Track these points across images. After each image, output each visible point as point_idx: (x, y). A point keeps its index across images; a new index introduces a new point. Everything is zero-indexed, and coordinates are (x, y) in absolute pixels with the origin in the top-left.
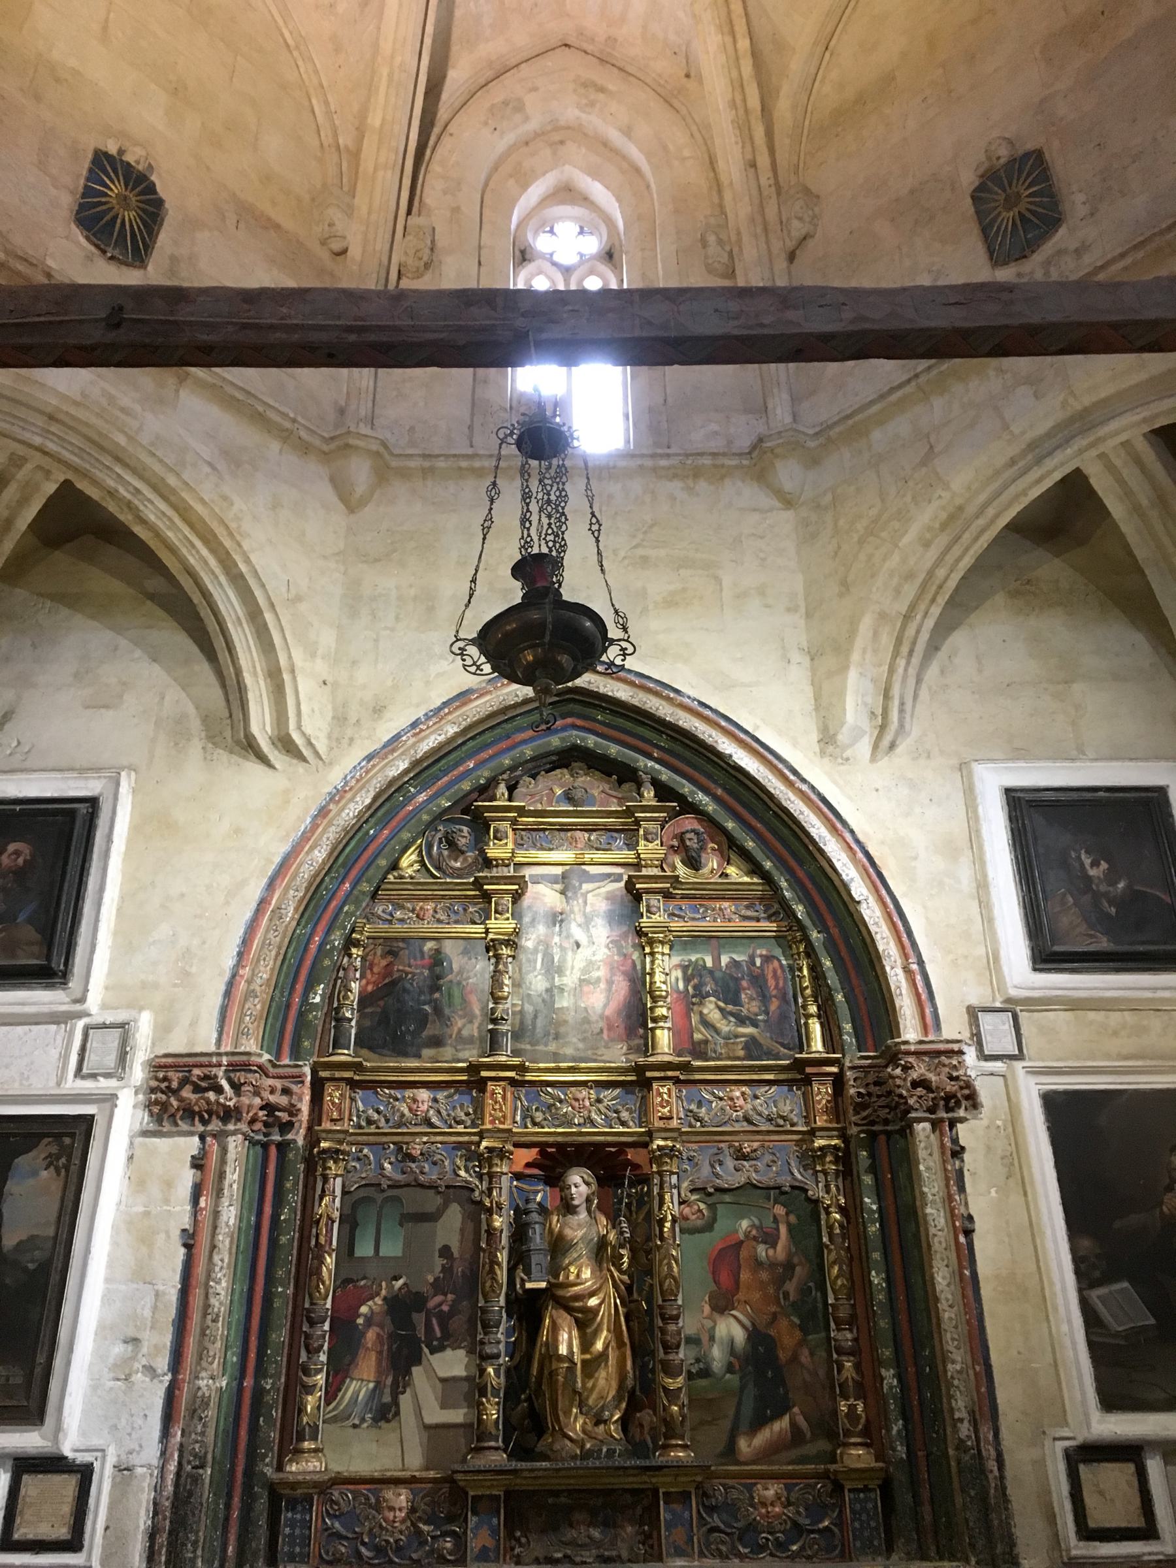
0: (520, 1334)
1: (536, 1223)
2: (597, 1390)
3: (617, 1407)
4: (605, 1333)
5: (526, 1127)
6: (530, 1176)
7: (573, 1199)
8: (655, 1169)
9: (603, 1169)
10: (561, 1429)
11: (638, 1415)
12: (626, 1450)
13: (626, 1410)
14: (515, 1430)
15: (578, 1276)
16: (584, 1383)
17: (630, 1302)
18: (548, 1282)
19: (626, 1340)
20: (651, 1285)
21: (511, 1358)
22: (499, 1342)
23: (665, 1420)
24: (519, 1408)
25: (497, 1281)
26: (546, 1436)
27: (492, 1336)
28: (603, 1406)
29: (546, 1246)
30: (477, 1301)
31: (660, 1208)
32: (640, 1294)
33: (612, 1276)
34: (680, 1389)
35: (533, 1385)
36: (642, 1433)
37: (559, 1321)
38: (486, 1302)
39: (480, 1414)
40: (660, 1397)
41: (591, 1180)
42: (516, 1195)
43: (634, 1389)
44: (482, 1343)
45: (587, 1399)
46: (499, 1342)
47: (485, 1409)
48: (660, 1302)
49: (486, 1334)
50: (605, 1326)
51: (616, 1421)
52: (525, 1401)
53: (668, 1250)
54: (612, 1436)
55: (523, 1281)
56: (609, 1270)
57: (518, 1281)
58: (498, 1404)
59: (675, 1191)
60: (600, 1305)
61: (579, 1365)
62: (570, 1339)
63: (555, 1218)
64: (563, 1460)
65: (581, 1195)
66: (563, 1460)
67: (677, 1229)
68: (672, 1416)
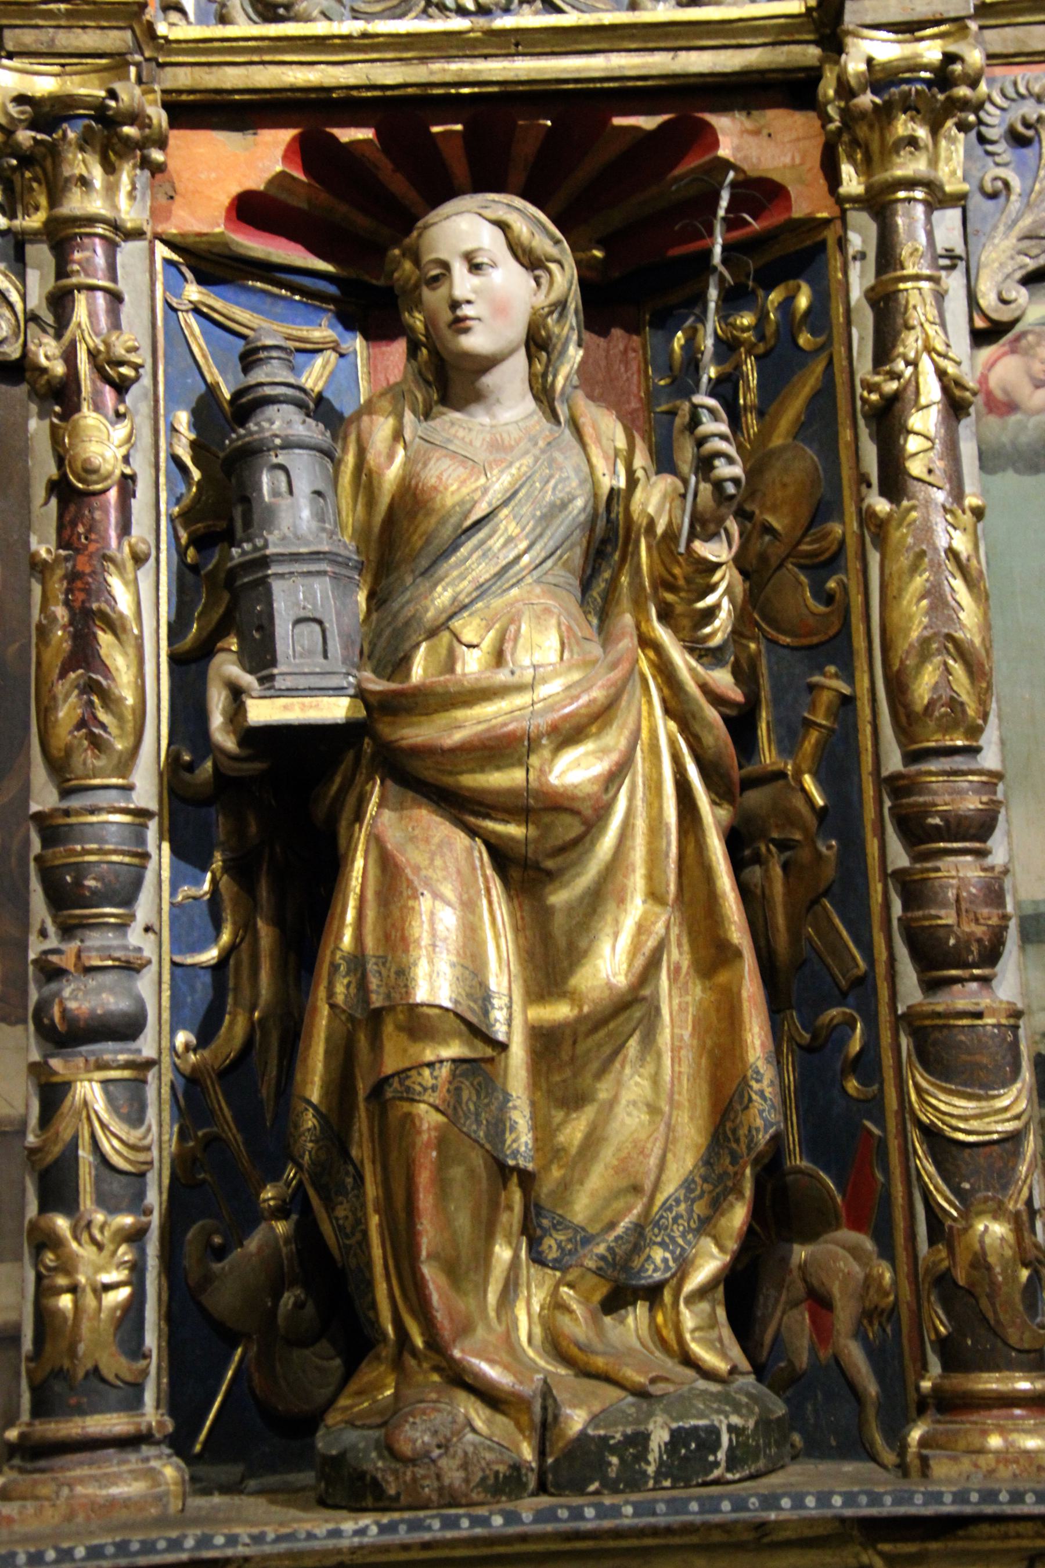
0: (246, 928)
1: (289, 445)
2: (608, 1155)
3: (705, 1226)
4: (636, 907)
5: (223, 19)
6: (266, 270)
7: (459, 325)
8: (852, 182)
9: (600, 244)
10: (436, 1345)
11: (801, 1253)
12: (765, 1424)
13: (750, 1238)
14: (231, 1339)
15: (499, 657)
16: (543, 1130)
17: (749, 783)
18: (361, 694)
19: (738, 933)
20: (847, 702)
21: (205, 1035)
22: (131, 967)
23: (943, 1281)
24: (253, 1244)
25: (109, 699)
26: (368, 1373)
27: (95, 939)
28: (639, 1228)
29: (347, 544)
30: (25, 793)
31: (883, 353)
32: (788, 744)
33: (665, 670)
34: (1014, 1139)
35: (307, 1147)
36: (822, 1331)
37: (412, 857)
38: (65, 793)
39: (44, 1290)
40: (911, 1177)
41: (542, 245)
42: (199, 346)
43: (777, 1141)
44: (52, 973)
45: (566, 1186)
46: (131, 967)
47: (67, 1266)
48: (894, 762)
49: (67, 931)
50: (637, 882)
51: (703, 1292)
52: (281, 1212)
53: (927, 530)
54: (688, 1360)
55: (237, 693)
56: (646, 642)
57: (217, 702)
58: (135, 1237)
59: (954, 282)
60: (614, 778)
61: (518, 1054)
62: (471, 933)
63: (382, 428)
64: (451, 1499)
65: (500, 309)
66: (451, 1499)
67: (968, 450)
68: (980, 1262)
